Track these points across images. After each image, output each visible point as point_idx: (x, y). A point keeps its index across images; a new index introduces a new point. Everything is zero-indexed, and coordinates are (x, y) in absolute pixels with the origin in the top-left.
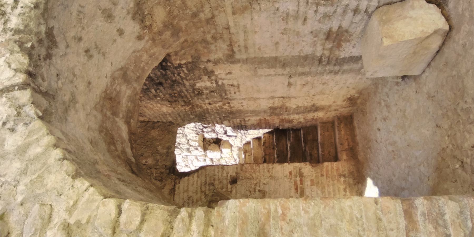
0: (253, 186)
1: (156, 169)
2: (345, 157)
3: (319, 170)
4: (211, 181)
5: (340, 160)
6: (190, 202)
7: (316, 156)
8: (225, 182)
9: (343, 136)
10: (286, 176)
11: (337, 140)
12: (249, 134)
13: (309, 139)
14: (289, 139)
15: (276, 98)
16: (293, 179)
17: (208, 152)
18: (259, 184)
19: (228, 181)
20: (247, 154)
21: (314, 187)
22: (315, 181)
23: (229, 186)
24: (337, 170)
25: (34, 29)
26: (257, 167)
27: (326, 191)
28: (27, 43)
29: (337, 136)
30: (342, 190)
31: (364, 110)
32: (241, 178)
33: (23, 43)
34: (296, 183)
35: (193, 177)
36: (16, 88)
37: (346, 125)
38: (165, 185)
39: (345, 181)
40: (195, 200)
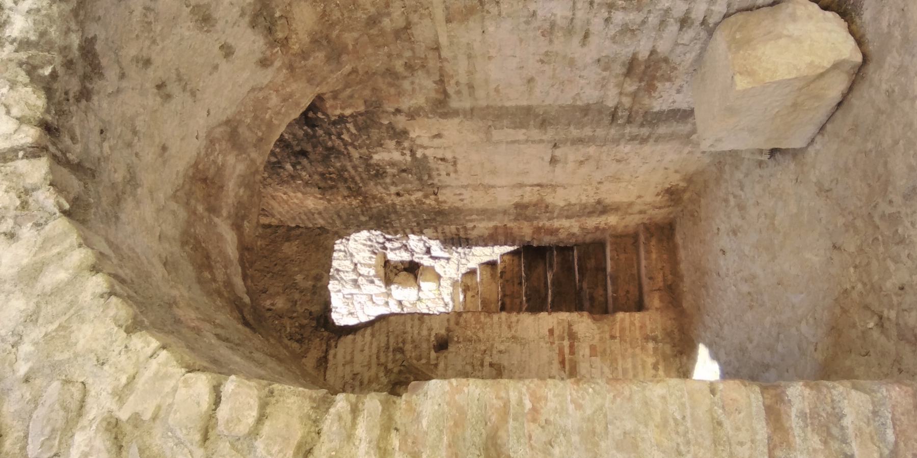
0: (478, 355)
1: (291, 318)
2: (656, 303)
3: (606, 328)
4: (397, 344)
5: (647, 309)
6: (357, 383)
7: (602, 299)
8: (425, 346)
9: (654, 262)
10: (544, 338)
11: (643, 271)
12: (473, 255)
13: (589, 266)
14: (551, 266)
15: (526, 186)
16: (557, 342)
17: (393, 287)
18: (491, 351)
19: (432, 346)
20: (469, 294)
21: (597, 360)
22: (598, 349)
23: (433, 354)
24: (641, 327)
25: (58, 40)
26: (488, 319)
27: (620, 369)
28: (42, 68)
29: (643, 263)
30: (649, 366)
31: (696, 214)
32: (456, 339)
33: (35, 68)
34: (561, 352)
35: (363, 336)
36: (21, 154)
37: (660, 241)
38: (307, 351)
39: (655, 350)
40: (366, 381)
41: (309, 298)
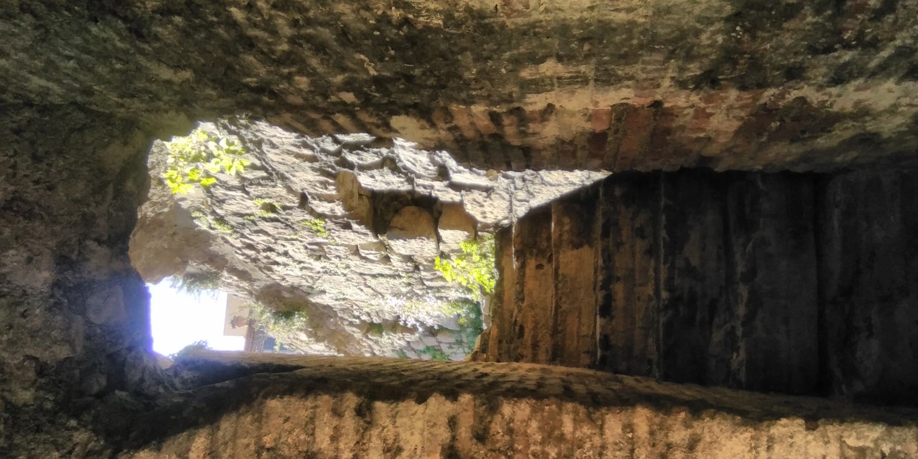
12: (543, 183)
26: (586, 430)
41: (38, 322)
